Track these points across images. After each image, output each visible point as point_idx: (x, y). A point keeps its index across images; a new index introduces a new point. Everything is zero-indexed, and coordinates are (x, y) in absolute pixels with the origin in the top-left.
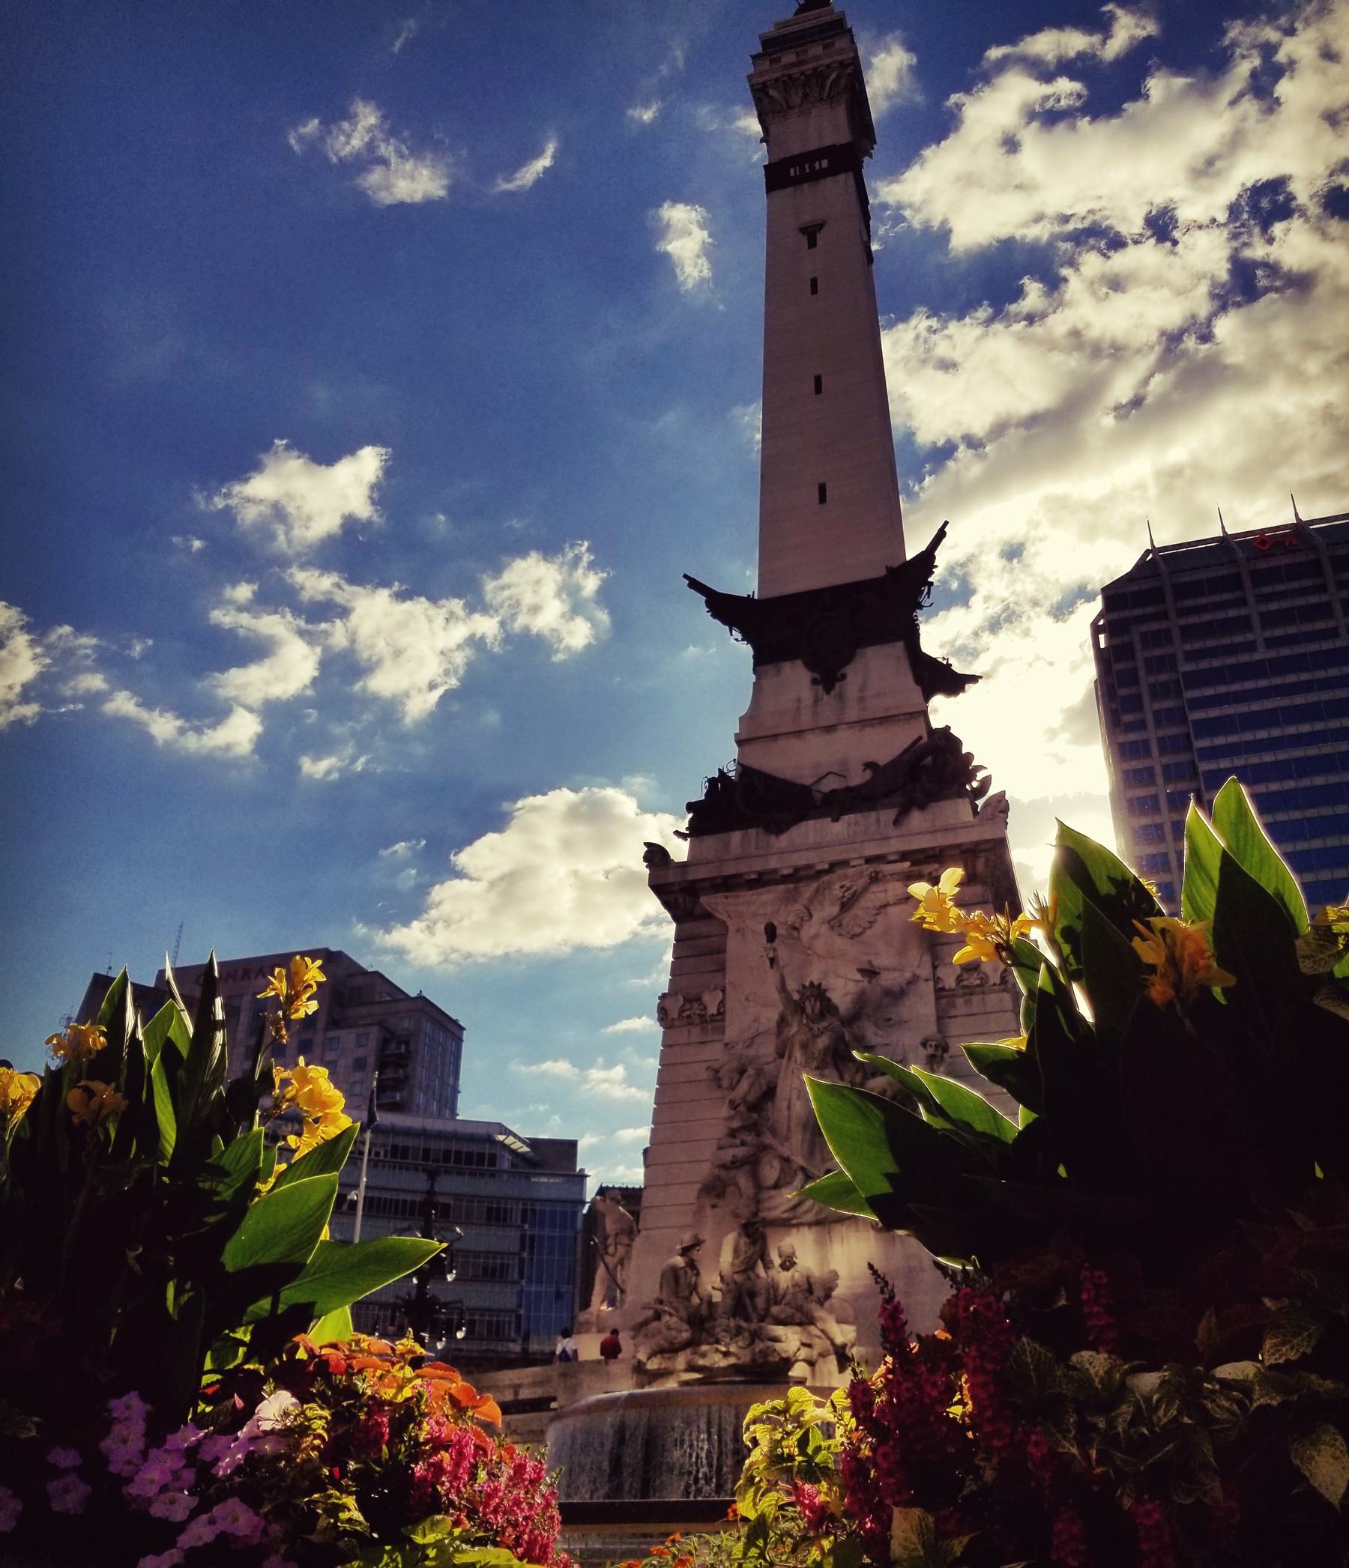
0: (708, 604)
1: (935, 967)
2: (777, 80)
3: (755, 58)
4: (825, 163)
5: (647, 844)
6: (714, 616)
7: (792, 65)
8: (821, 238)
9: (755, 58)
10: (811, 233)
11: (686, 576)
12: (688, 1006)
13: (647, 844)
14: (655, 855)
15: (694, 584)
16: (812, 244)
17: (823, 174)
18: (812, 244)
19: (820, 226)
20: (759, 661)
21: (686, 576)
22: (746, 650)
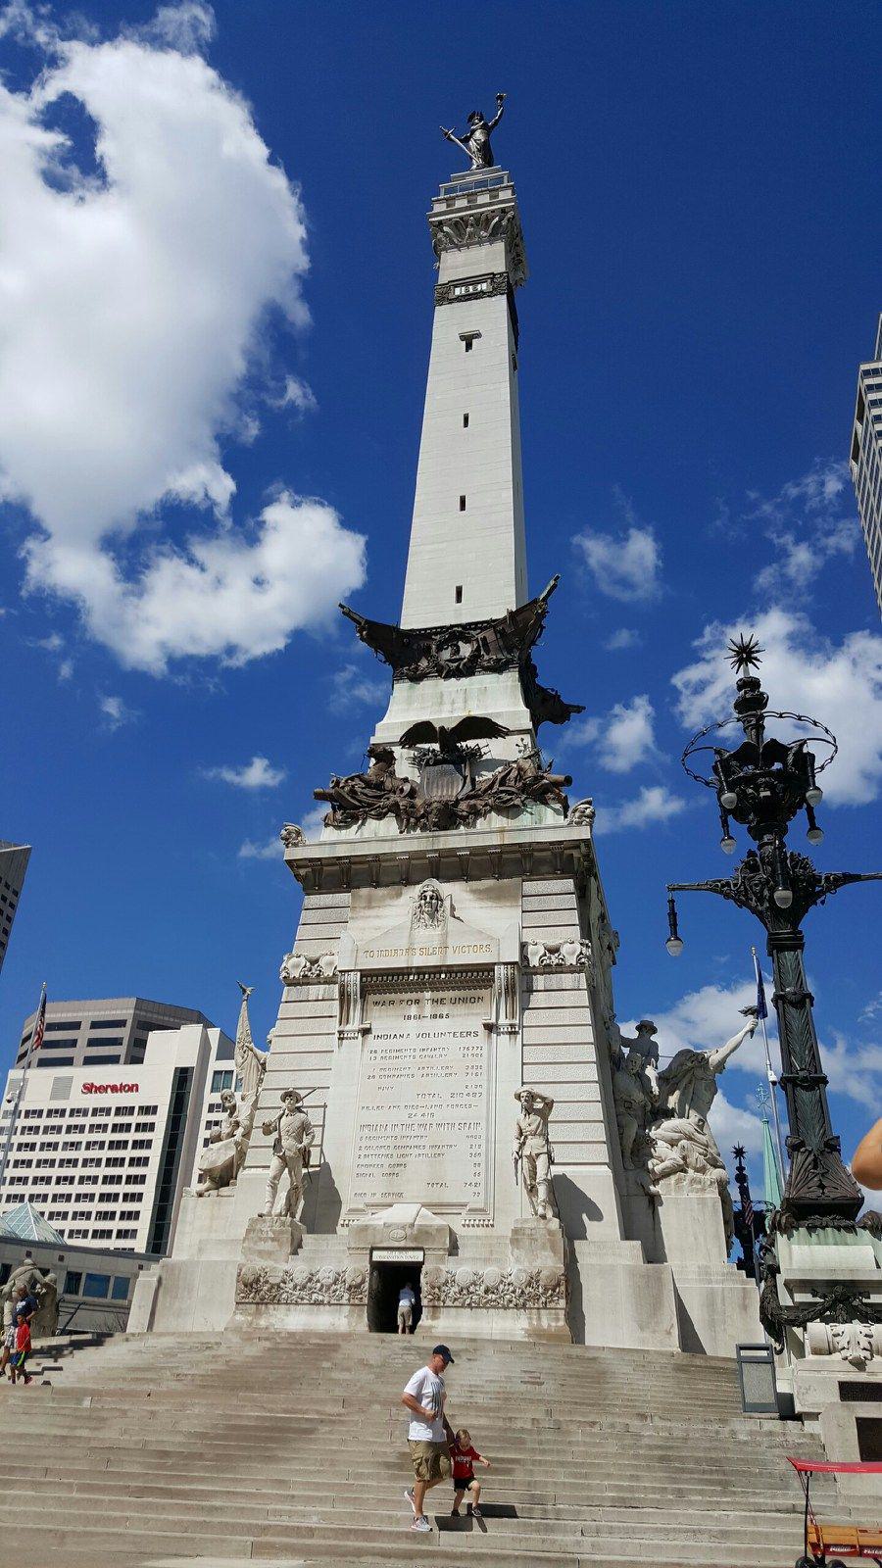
2: (450, 219)
8: (475, 342)
16: (469, 346)
19: (478, 336)
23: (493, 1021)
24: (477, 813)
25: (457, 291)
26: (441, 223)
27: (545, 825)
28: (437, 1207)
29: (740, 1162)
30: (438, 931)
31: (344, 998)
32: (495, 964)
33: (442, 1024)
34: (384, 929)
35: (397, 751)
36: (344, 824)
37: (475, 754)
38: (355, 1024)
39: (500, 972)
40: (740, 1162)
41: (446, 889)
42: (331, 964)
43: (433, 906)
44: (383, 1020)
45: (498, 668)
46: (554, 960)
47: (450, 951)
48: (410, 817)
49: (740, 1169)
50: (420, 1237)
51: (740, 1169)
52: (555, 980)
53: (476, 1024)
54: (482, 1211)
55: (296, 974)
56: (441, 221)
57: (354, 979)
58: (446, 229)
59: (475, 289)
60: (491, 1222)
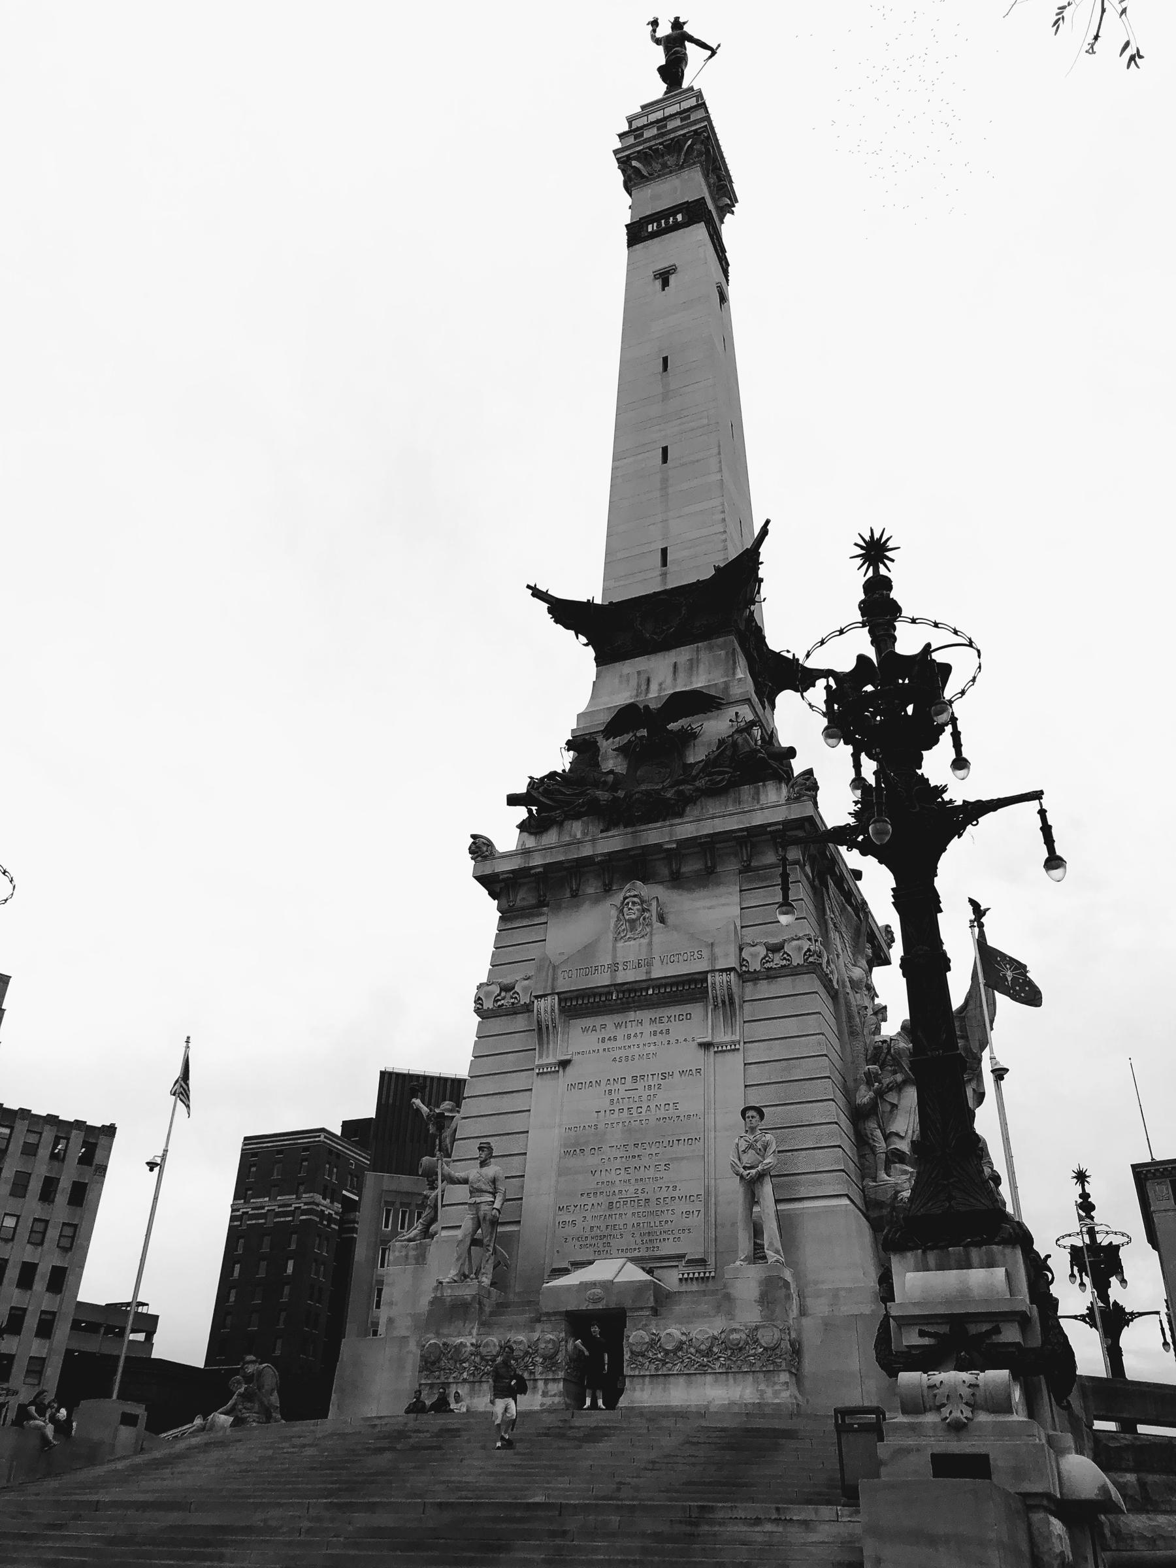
0: (550, 611)
1: (741, 950)
2: (638, 152)
3: (621, 136)
4: (679, 217)
5: (474, 837)
6: (556, 622)
7: (654, 137)
8: (672, 279)
9: (621, 136)
10: (664, 277)
11: (529, 587)
12: (503, 994)
13: (474, 837)
14: (480, 848)
15: (537, 593)
16: (665, 283)
17: (677, 226)
19: (672, 270)
20: (600, 661)
21: (529, 587)
22: (590, 652)
23: (708, 1039)
29: (1083, 1189)
30: (644, 941)
32: (707, 972)
40: (1083, 1189)
42: (525, 989)
46: (777, 960)
47: (657, 962)
48: (613, 815)
49: (1085, 1196)
51: (1085, 1196)
52: (784, 986)
54: (702, 1262)
55: (488, 1004)
56: (627, 156)
58: (634, 163)
59: (667, 222)
60: (713, 1274)
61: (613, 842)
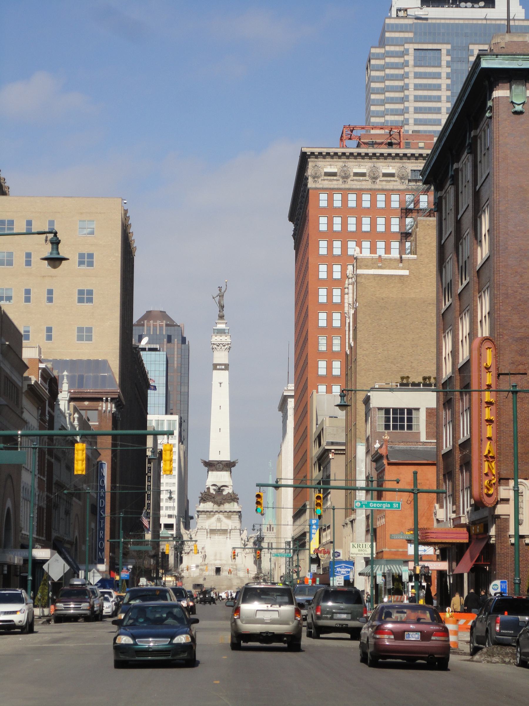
10: (221, 383)
18: (220, 386)
24: (224, 503)
25: (218, 367)
26: (214, 344)
27: (235, 507)
28: (221, 560)
31: (207, 532)
33: (221, 537)
34: (212, 523)
35: (210, 487)
36: (204, 503)
37: (224, 489)
38: (209, 536)
39: (229, 530)
41: (221, 516)
43: (219, 520)
44: (212, 536)
45: (226, 471)
48: (215, 502)
50: (221, 565)
53: (225, 537)
57: (209, 530)
61: (216, 508)
